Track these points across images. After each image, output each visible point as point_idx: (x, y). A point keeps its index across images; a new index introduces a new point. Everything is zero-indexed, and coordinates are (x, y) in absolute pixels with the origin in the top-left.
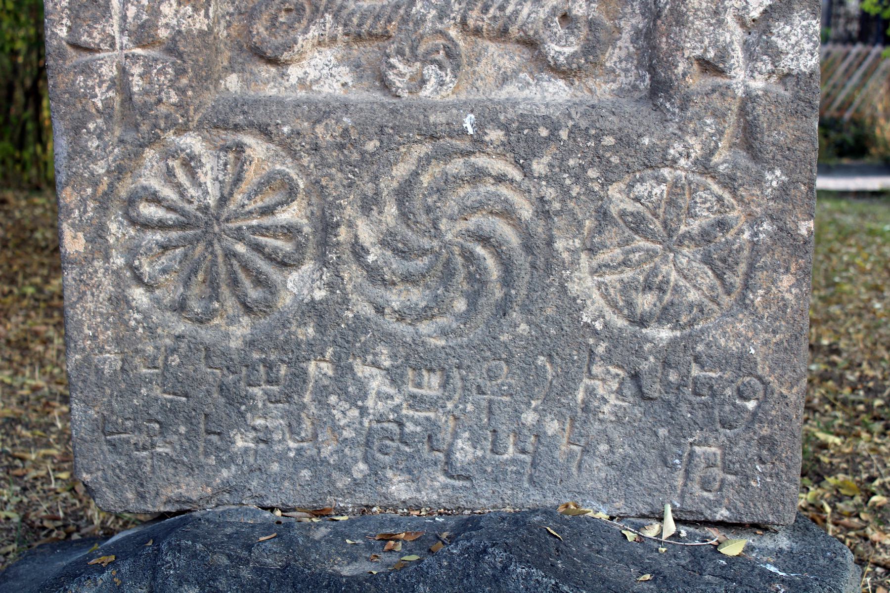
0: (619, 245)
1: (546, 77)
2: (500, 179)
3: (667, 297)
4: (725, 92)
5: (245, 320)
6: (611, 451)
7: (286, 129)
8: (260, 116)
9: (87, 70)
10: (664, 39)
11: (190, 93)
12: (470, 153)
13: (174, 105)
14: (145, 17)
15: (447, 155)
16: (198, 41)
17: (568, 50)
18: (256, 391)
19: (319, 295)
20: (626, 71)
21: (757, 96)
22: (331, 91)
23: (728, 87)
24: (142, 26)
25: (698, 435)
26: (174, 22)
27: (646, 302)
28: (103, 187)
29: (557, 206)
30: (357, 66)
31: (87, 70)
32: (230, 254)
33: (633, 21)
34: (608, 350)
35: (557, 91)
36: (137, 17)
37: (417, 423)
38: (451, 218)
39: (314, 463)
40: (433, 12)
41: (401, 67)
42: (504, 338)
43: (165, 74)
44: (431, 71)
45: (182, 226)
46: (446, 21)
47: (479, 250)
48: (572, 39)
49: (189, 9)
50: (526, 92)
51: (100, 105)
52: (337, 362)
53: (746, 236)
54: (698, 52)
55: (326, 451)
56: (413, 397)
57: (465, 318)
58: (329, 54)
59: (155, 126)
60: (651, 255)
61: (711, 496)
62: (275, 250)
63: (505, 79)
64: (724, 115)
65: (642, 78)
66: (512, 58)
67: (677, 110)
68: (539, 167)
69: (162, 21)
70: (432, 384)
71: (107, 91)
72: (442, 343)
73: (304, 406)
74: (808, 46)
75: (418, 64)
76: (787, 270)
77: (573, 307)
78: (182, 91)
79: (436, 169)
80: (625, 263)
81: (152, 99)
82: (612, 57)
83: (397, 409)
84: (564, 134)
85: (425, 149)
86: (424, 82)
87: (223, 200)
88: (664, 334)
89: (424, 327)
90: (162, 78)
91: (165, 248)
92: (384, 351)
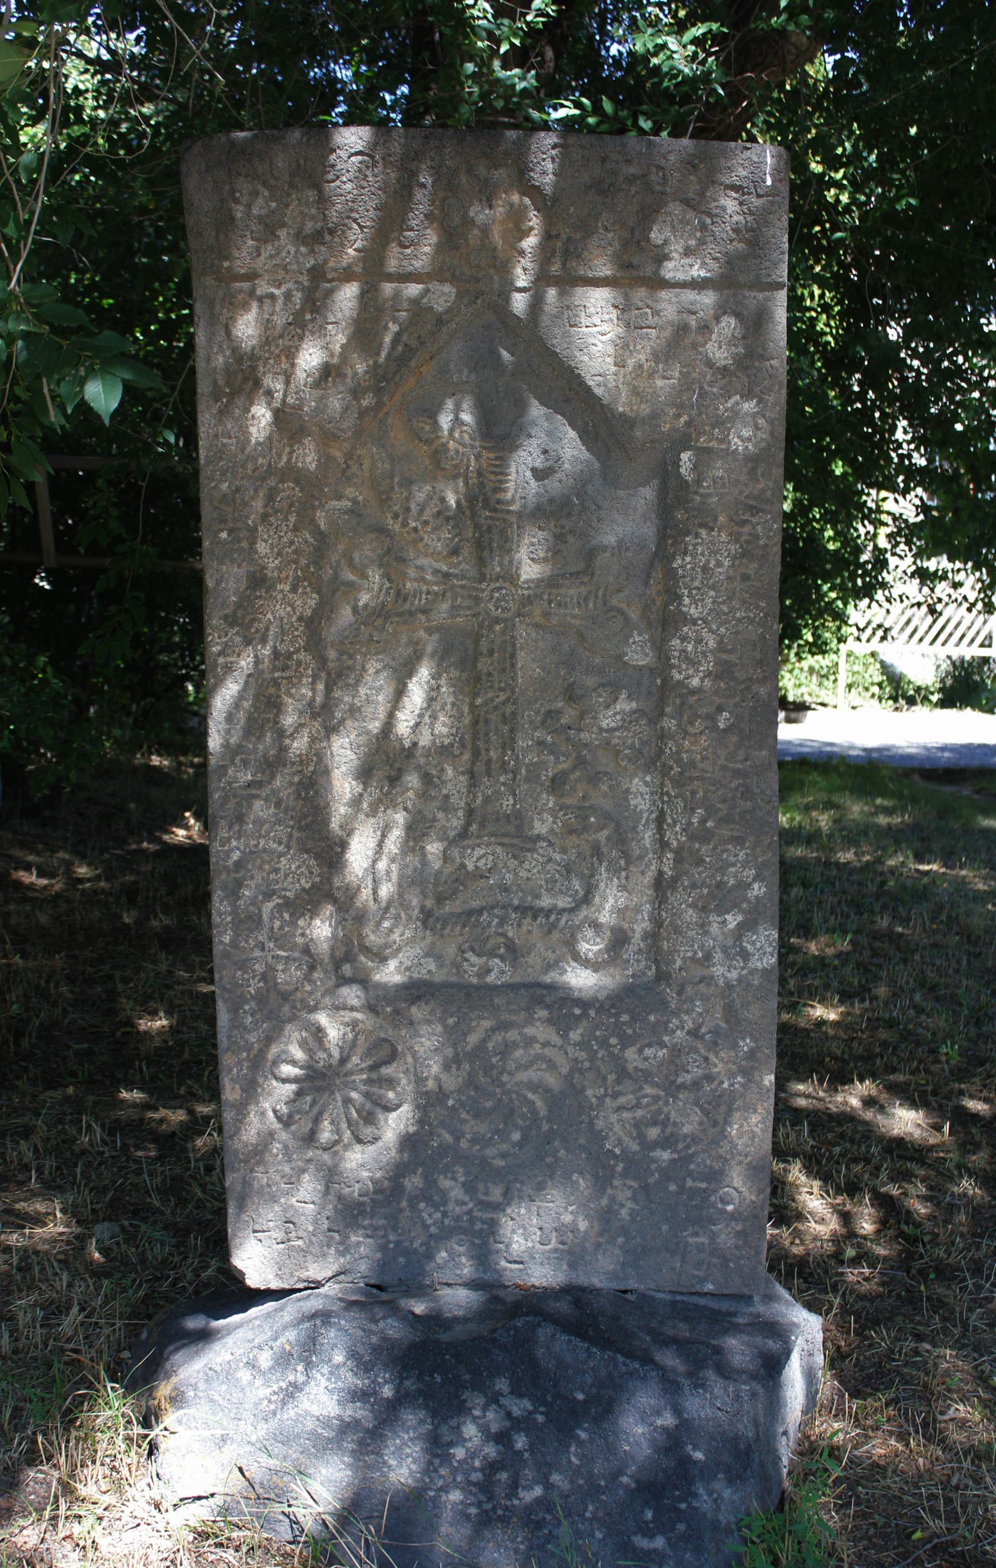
0: (633, 1092)
3: (669, 1130)
4: (708, 980)
6: (626, 1242)
17: (596, 948)
20: (638, 961)
23: (712, 977)
27: (653, 1133)
28: (255, 1052)
29: (587, 1064)
31: (244, 965)
34: (625, 1169)
37: (484, 1222)
38: (510, 1073)
39: (407, 1252)
41: (473, 958)
47: (530, 1096)
52: (425, 1177)
53: (726, 1085)
55: (416, 1244)
56: (481, 1203)
57: (520, 1144)
59: (294, 1007)
60: (656, 1099)
61: (701, 1274)
65: (649, 968)
68: (575, 1036)
73: (401, 1210)
74: (769, 950)
76: (755, 1111)
79: (498, 1037)
82: (629, 952)
83: (469, 1212)
86: (489, 971)
87: (343, 1061)
88: (666, 1155)
89: (490, 1152)
92: (460, 1170)
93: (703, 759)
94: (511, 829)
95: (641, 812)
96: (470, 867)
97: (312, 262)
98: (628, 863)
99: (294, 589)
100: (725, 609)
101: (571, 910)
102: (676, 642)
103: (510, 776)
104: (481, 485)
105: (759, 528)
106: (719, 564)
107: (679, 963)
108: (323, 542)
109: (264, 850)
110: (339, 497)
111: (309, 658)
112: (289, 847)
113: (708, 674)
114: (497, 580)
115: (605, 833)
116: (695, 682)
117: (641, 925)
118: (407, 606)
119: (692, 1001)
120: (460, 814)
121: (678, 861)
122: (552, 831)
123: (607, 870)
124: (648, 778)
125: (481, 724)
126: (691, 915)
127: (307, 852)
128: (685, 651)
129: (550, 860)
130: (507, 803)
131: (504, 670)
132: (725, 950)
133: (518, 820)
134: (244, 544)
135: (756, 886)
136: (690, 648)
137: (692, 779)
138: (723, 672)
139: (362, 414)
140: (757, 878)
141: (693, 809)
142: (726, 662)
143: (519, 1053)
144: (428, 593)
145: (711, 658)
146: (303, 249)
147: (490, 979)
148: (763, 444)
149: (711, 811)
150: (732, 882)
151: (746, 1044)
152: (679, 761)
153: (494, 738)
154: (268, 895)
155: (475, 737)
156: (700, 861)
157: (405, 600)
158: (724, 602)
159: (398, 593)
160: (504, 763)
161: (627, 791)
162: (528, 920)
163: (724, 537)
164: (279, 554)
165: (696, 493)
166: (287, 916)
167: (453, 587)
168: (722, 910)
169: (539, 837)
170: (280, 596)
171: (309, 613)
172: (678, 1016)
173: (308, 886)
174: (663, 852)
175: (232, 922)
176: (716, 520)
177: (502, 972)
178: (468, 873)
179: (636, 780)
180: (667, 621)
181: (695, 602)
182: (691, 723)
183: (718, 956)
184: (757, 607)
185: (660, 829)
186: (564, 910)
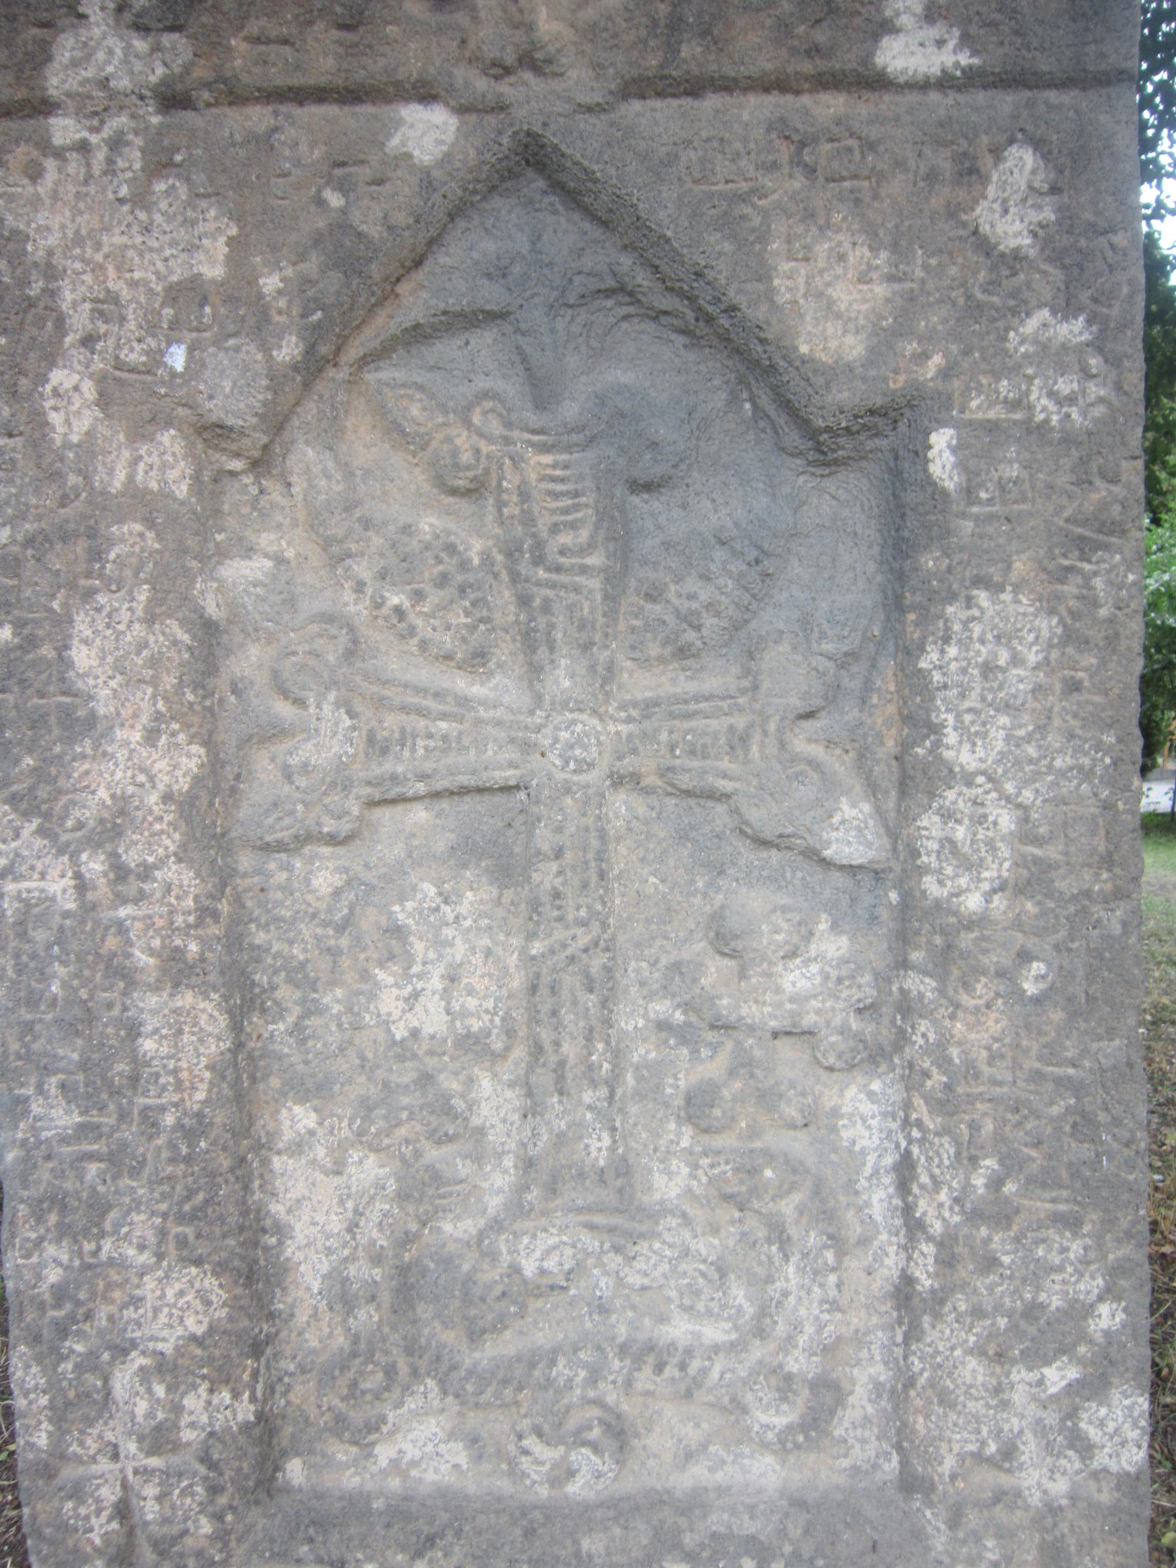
1: (747, 1451)
9: (77, 1492)
10: (921, 1420)
11: (229, 1518)
13: (207, 1536)
14: (160, 1415)
16: (242, 1440)
20: (864, 1441)
21: (1061, 1508)
22: (437, 1478)
23: (1018, 1494)
24: (158, 1428)
26: (204, 1419)
30: (473, 1441)
31: (77, 1492)
33: (872, 1371)
36: (150, 1415)
40: (583, 1374)
43: (193, 1495)
44: (582, 1457)
46: (601, 1385)
48: (785, 1407)
49: (226, 1396)
50: (719, 1476)
51: (98, 1541)
54: (972, 1447)
58: (432, 1427)
63: (689, 1456)
64: (1013, 1535)
66: (697, 1426)
67: (943, 1527)
69: (185, 1419)
71: (109, 1522)
75: (562, 1449)
78: (218, 1517)
81: (175, 1530)
86: (571, 1474)
90: (188, 1501)
93: (991, 1061)
94: (608, 1196)
95: (863, 1153)
96: (529, 1268)
97: (160, 71)
98: (841, 1254)
99: (151, 737)
100: (1031, 751)
101: (732, 1347)
102: (930, 822)
103: (604, 1092)
104: (528, 520)
105: (1098, 583)
106: (1016, 660)
107: (949, 1464)
108: (210, 639)
109: (111, 1262)
110: (249, 551)
112: (160, 1257)
114: (565, 705)
115: (796, 1198)
116: (973, 902)
117: (867, 1374)
118: (389, 766)
119: (978, 1540)
120: (509, 1162)
121: (947, 1260)
122: (689, 1191)
123: (801, 1271)
124: (876, 1086)
125: (544, 991)
126: (973, 1370)
127: (198, 1262)
128: (951, 842)
129: (686, 1252)
130: (598, 1147)
131: (585, 885)
132: (1040, 1429)
133: (622, 1172)
134: (47, 651)
135: (1104, 1309)
136: (961, 833)
137: (971, 1099)
138: (1031, 880)
139: (276, 379)
141: (974, 1161)
142: (1036, 861)
144: (430, 736)
145: (1004, 851)
146: (140, 45)
147: (575, 1488)
148: (1099, 411)
149: (1011, 1163)
150: (1056, 1302)
152: (944, 1062)
153: (567, 1016)
154: (122, 1351)
155: (534, 1019)
156: (990, 1263)
157: (384, 751)
158: (1029, 738)
159: (371, 739)
160: (590, 1067)
161: (835, 1113)
162: (647, 1371)
164: (119, 668)
165: (964, 515)
166: (160, 1391)
167: (478, 722)
168: (1037, 1357)
169: (664, 1210)
171: (184, 784)
173: (200, 1330)
174: (912, 1238)
175: (51, 1406)
176: (1009, 567)
177: (599, 1475)
178: (525, 1282)
179: (852, 1091)
180: (912, 780)
181: (969, 737)
182: (967, 986)
183: (1029, 1448)
184: (1099, 746)
186: (716, 1348)
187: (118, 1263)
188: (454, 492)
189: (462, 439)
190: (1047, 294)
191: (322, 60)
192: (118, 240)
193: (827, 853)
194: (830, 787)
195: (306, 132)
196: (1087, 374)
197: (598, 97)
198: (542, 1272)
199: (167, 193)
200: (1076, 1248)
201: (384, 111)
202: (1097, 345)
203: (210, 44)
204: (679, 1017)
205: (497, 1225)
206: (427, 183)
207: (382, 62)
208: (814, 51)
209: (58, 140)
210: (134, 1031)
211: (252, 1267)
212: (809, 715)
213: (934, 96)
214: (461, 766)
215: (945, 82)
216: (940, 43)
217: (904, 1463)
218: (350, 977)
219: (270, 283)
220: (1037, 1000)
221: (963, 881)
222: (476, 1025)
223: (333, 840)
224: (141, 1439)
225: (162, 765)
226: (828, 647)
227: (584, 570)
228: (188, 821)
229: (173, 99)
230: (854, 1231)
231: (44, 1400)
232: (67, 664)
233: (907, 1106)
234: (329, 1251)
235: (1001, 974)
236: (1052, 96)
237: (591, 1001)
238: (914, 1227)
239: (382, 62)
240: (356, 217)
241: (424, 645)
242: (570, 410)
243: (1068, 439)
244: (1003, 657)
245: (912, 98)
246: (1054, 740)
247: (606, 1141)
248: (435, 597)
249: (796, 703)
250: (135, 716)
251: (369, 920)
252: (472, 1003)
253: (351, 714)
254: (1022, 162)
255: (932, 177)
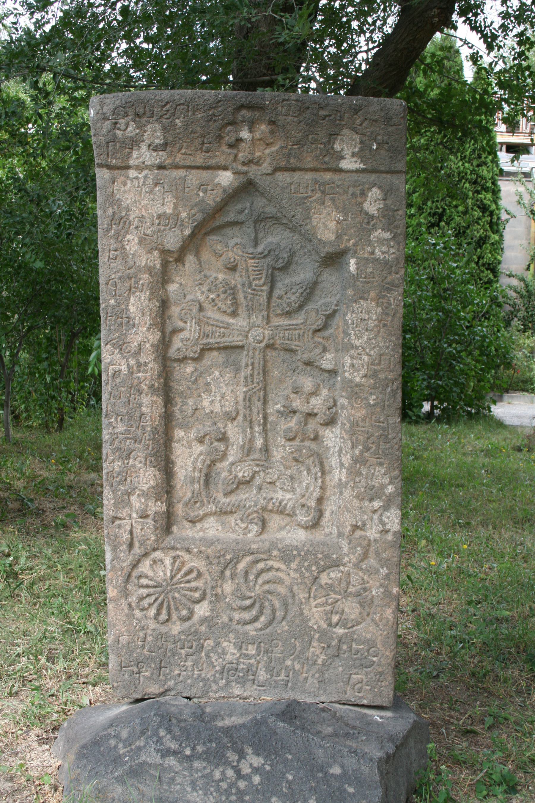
2: (278, 570)
5: (178, 623)
7: (196, 550)
8: (186, 544)
12: (266, 560)
15: (257, 562)
17: (305, 519)
18: (183, 651)
19: (207, 614)
25: (355, 671)
30: (223, 524)
32: (174, 598)
34: (319, 637)
35: (302, 535)
42: (279, 631)
45: (155, 587)
50: (289, 535)
53: (374, 593)
54: (354, 523)
55: (209, 676)
62: (191, 596)
63: (281, 528)
68: (293, 565)
70: (252, 650)
72: (254, 633)
76: (389, 607)
77: (305, 620)
80: (326, 603)
84: (303, 553)
85: (249, 559)
87: (172, 578)
89: (249, 627)
91: (148, 595)
96: (240, 475)
99: (149, 329)
105: (392, 299)
110: (173, 282)
111: (156, 366)
112: (145, 464)
113: (366, 376)
115: (312, 458)
116: (358, 380)
127: (154, 467)
134: (123, 307)
135: (390, 487)
140: (391, 483)
142: (375, 370)
143: (264, 574)
146: (155, 154)
151: (384, 571)
161: (323, 437)
163: (374, 304)
166: (143, 500)
168: (371, 500)
170: (141, 334)
172: (348, 555)
179: (327, 431)
185: (340, 456)
187: (134, 466)
188: (228, 268)
189: (230, 254)
190: (381, 226)
191: (199, 160)
192: (145, 202)
193: (323, 366)
194: (325, 350)
195: (194, 178)
196: (390, 247)
197: (269, 172)
198: (244, 477)
199: (159, 190)
200: (383, 471)
201: (215, 172)
202: (394, 238)
203: (170, 154)
204: (282, 409)
205: (233, 464)
206: (225, 190)
207: (215, 161)
208: (325, 162)
209: (131, 176)
210: (141, 405)
211: (167, 470)
212: (319, 330)
213: (354, 174)
214: (227, 341)
215: (357, 171)
216: (356, 162)
217: (338, 530)
218: (195, 395)
219: (184, 215)
220: (373, 405)
221: (356, 374)
222: (228, 409)
223: (194, 359)
224: (137, 513)
225: (151, 337)
226: (325, 313)
227: (262, 291)
228: (157, 351)
229: (161, 167)
230: (327, 468)
231: (112, 502)
232: (128, 310)
233: (341, 433)
234: (186, 470)
235: (365, 398)
236: (384, 175)
237: (260, 404)
238: (342, 465)
239: (215, 161)
240: (206, 199)
241: (219, 309)
242: (260, 249)
243: (386, 262)
244: (367, 317)
245: (348, 174)
246: (379, 339)
247: (262, 441)
248: (222, 296)
249: (315, 327)
250: (146, 323)
251: (201, 381)
252: (227, 403)
253: (199, 326)
254: (375, 193)
255: (354, 195)
